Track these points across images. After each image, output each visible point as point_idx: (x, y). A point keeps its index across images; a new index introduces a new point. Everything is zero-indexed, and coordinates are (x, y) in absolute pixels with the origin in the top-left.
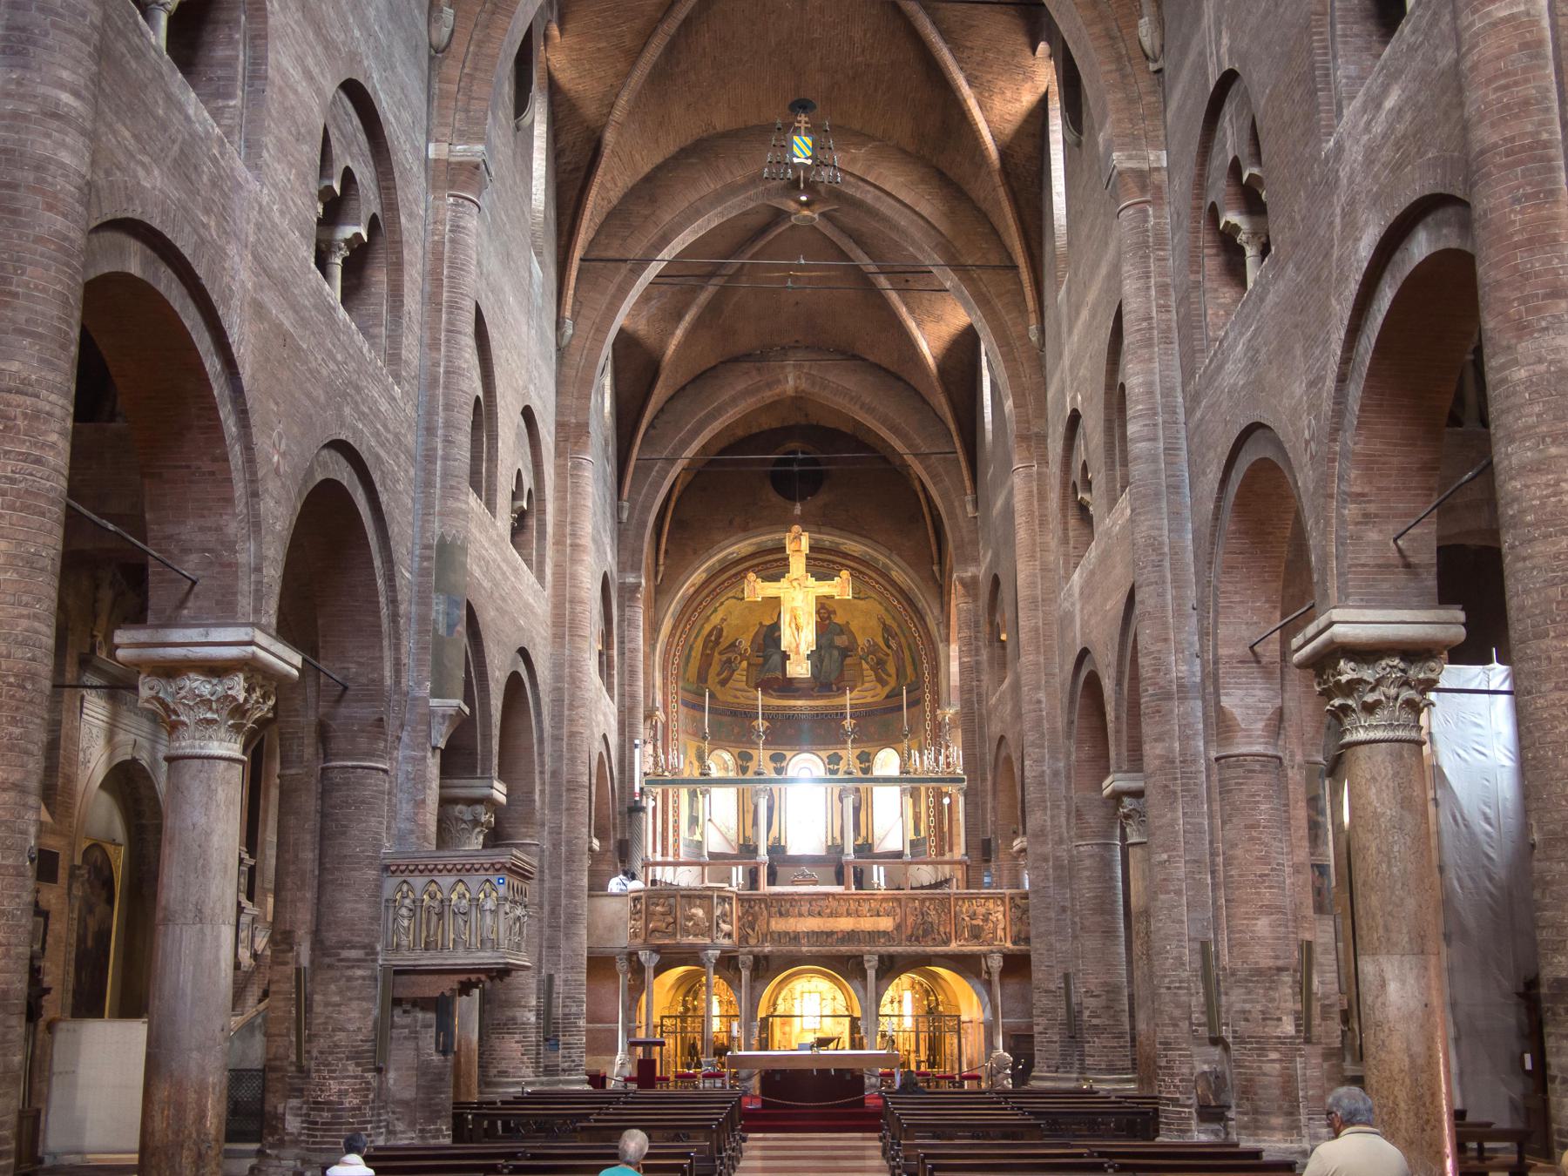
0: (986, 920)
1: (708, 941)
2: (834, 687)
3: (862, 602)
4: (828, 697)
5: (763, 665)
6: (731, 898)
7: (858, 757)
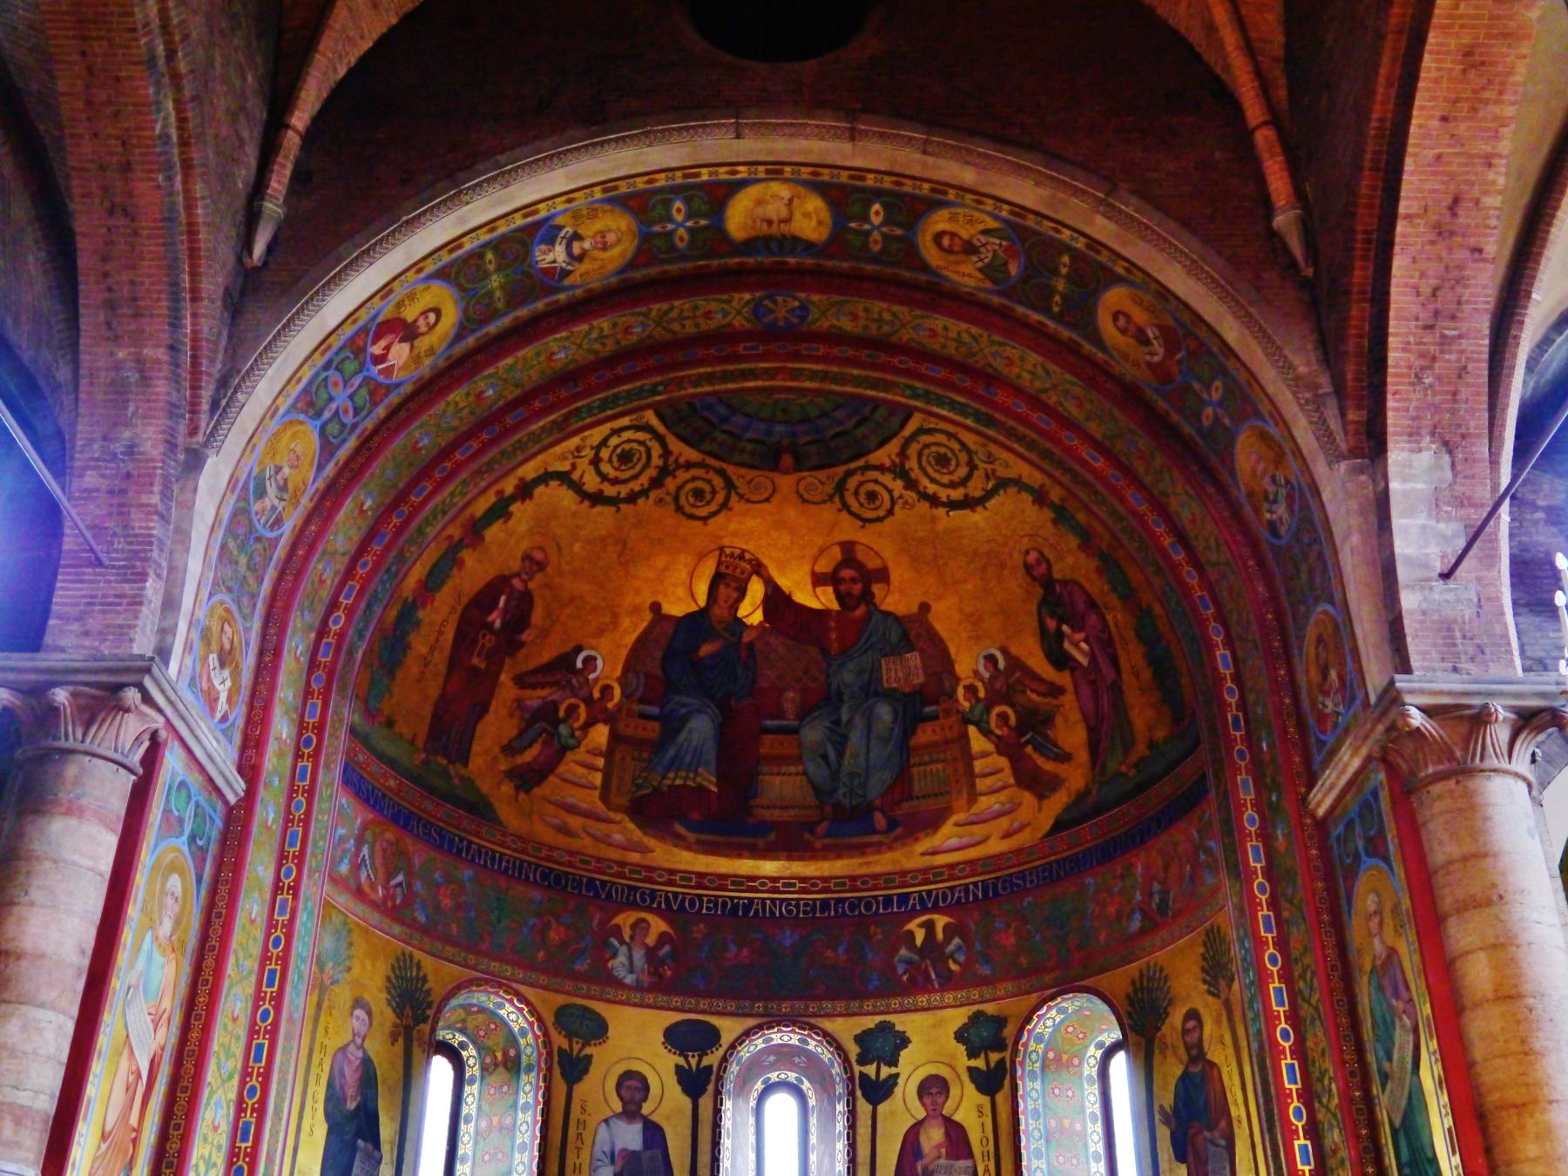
2: (880, 820)
3: (977, 517)
4: (861, 850)
5: (659, 746)
7: (960, 1036)
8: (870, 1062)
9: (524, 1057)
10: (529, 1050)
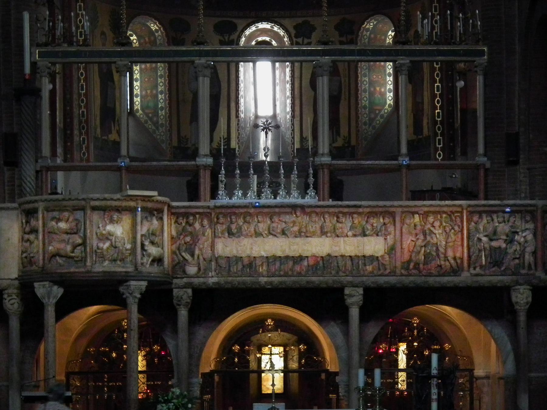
0: (510, 241)
1: (131, 269)
6: (160, 211)
8: (300, 38)
9: (158, 41)
10: (159, 38)
